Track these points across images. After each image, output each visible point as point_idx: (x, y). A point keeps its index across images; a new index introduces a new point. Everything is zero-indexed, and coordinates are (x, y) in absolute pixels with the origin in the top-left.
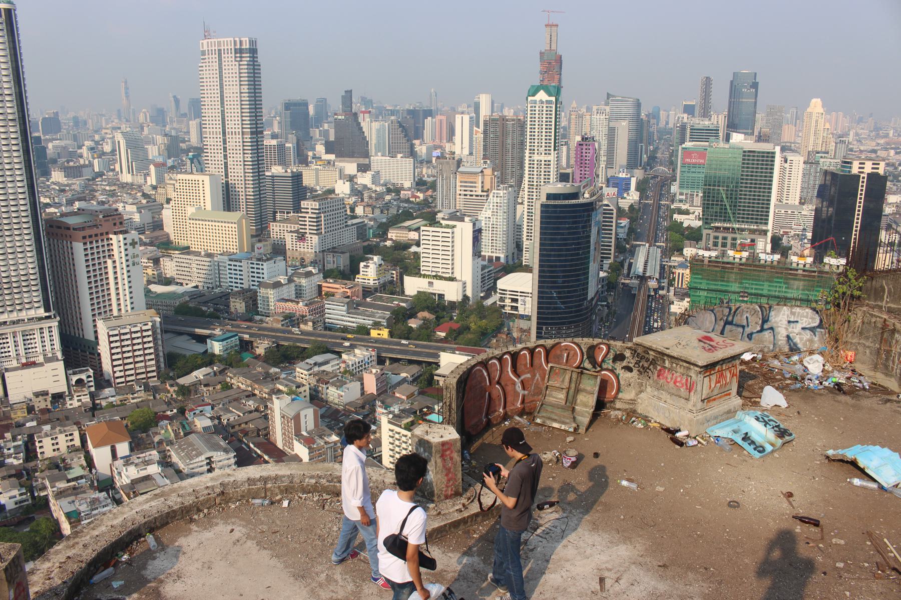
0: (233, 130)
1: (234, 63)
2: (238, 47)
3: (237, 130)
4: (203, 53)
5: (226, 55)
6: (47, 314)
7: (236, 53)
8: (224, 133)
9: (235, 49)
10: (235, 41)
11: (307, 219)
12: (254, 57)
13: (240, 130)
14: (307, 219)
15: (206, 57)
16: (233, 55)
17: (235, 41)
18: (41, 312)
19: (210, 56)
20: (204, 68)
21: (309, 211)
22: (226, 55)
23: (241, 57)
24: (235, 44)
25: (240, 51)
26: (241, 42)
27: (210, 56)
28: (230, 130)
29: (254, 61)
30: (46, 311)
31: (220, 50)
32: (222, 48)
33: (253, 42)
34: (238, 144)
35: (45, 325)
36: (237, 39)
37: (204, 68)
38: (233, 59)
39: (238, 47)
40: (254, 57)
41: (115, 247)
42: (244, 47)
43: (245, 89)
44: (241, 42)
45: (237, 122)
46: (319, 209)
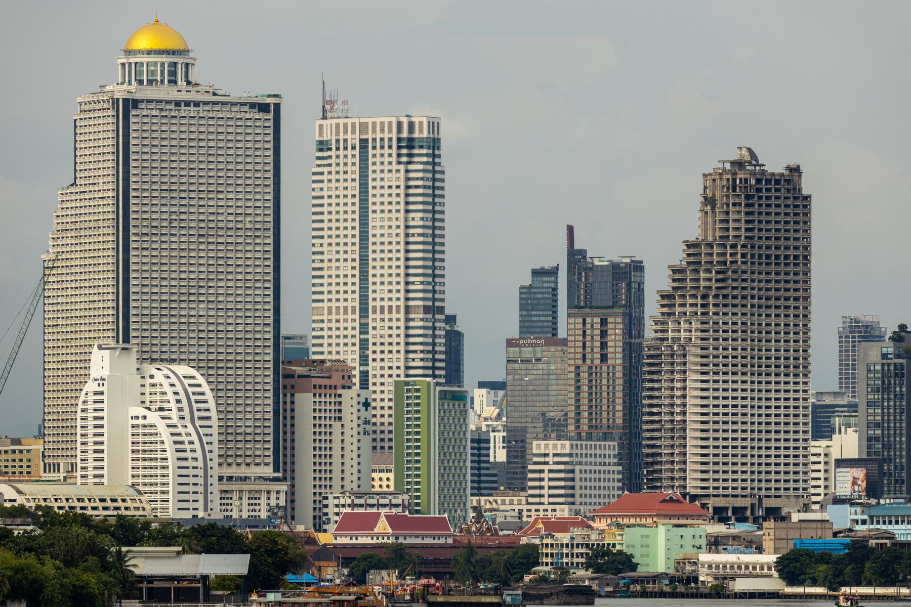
0: (386, 304)
1: (394, 167)
2: (405, 134)
3: (394, 304)
4: (323, 146)
5: (378, 151)
6: (276, 475)
7: (399, 148)
8: (364, 312)
9: (399, 140)
10: (400, 124)
11: (545, 475)
12: (434, 156)
13: (402, 303)
14: (545, 475)
15: (333, 153)
16: (394, 151)
17: (400, 124)
18: (268, 471)
19: (341, 152)
20: (325, 177)
21: (550, 459)
22: (378, 151)
23: (410, 155)
24: (400, 130)
25: (411, 143)
26: (411, 125)
27: (341, 152)
28: (378, 304)
29: (434, 164)
30: (274, 471)
31: (364, 143)
32: (370, 136)
33: (434, 126)
34: (394, 332)
35: (275, 487)
36: (405, 121)
37: (325, 177)
38: (394, 159)
39: (405, 134)
40: (434, 156)
41: (345, 407)
42: (416, 135)
43: (417, 219)
44: (411, 125)
45: (394, 287)
46: (570, 455)
